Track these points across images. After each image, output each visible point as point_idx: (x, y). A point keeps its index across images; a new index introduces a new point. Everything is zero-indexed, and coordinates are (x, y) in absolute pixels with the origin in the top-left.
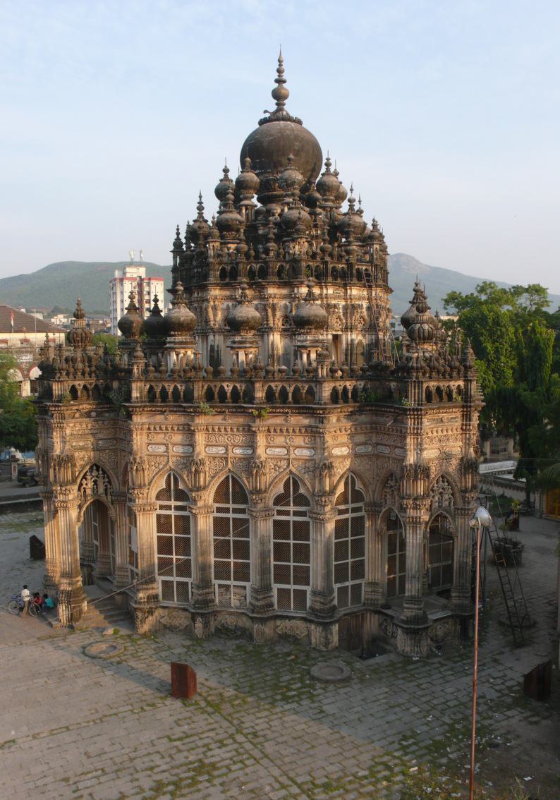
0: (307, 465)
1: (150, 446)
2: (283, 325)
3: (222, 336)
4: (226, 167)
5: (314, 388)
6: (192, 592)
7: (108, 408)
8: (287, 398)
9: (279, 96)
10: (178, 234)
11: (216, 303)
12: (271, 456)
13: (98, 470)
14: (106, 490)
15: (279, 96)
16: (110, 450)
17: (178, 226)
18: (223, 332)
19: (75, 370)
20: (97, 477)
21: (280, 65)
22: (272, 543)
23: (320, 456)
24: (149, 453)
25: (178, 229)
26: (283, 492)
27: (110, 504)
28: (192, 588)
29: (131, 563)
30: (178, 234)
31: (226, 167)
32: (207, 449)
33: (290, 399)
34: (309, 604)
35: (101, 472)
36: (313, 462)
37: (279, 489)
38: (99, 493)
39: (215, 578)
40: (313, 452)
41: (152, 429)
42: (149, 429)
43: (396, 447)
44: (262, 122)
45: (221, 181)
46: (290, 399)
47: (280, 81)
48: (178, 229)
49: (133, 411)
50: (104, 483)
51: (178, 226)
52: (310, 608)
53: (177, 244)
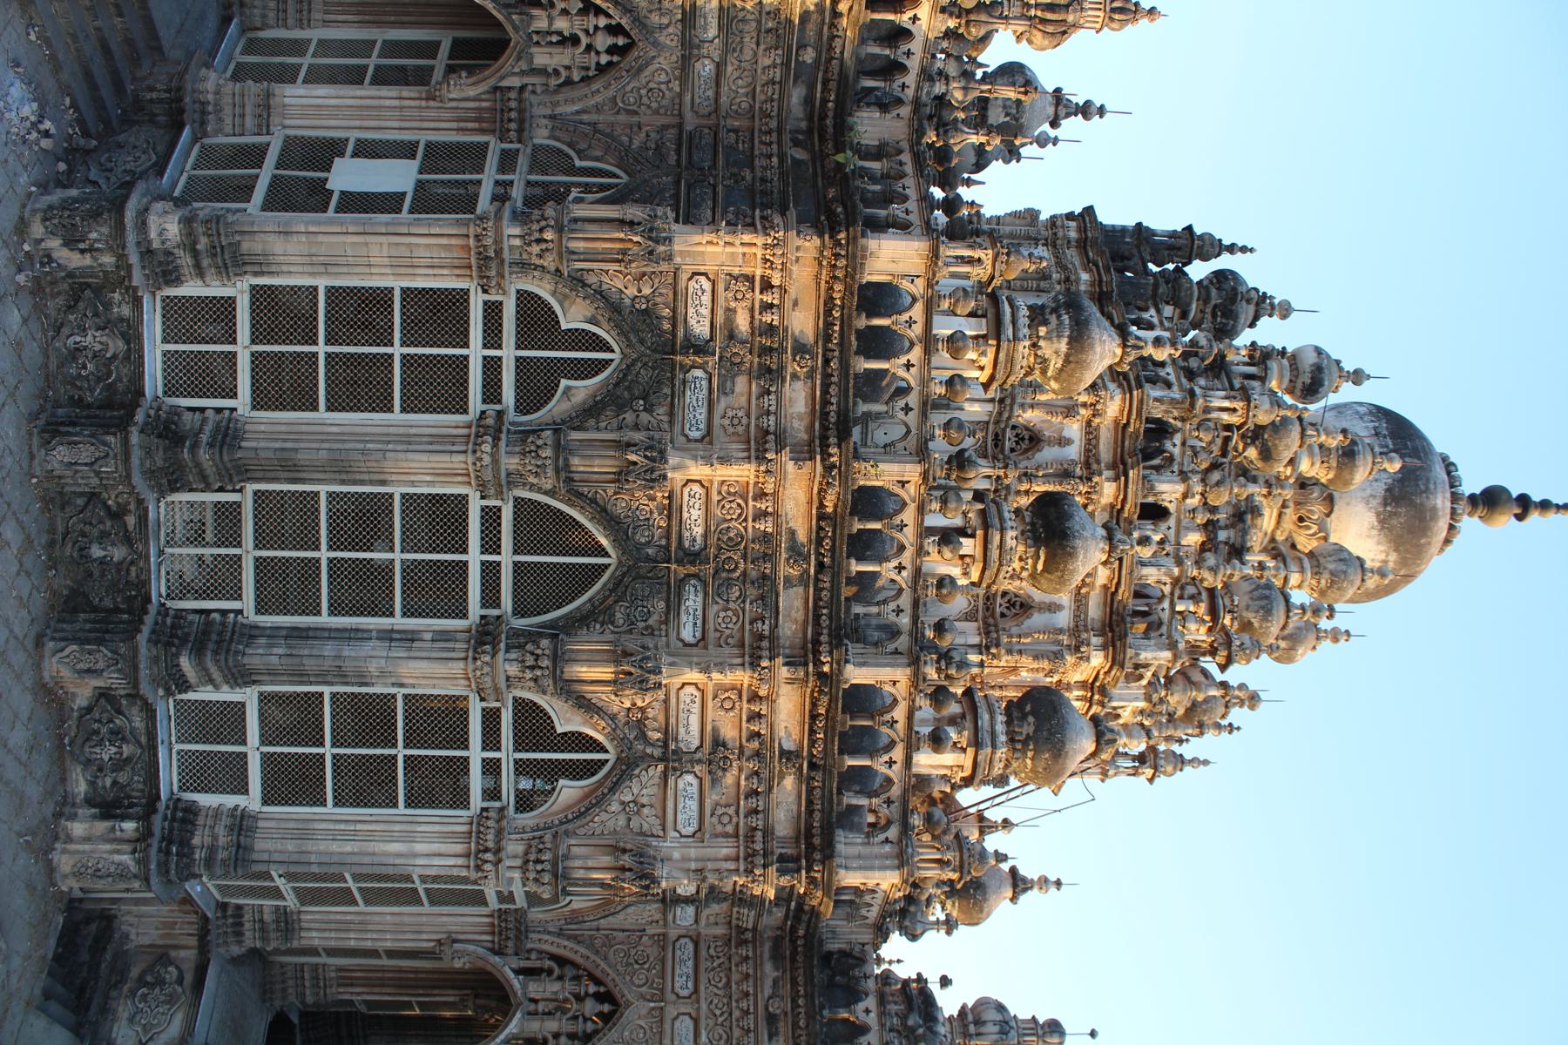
0: (646, 811)
1: (707, 285)
2: (1004, 594)
3: (986, 419)
4: (1369, 377)
5: (882, 837)
6: (202, 410)
7: (824, 101)
8: (854, 752)
9: (1490, 500)
10: (1231, 249)
11: (1083, 411)
12: (673, 700)
13: (611, 50)
14: (543, 72)
15: (1490, 500)
16: (680, 95)
17: (1251, 250)
18: (997, 422)
19: (969, 12)
20: (589, 48)
21: (1558, 507)
22: (393, 690)
23: (676, 855)
24: (684, 277)
25: (1244, 249)
26: (560, 730)
27: (492, 82)
28: (219, 410)
29: (290, 144)
30: (1231, 249)
31: (1369, 377)
32: (696, 488)
33: (851, 762)
34: (206, 800)
35: (604, 59)
36: (658, 831)
37: (569, 721)
38: (534, 50)
39: (256, 493)
40: (690, 830)
41: (768, 298)
42: (767, 286)
43: (696, 1021)
44: (1449, 467)
45: (1338, 362)
46: (851, 762)
47: (1524, 505)
48: (1244, 249)
49: (838, 243)
50: (568, 68)
51: (1251, 250)
52: (192, 810)
53: (1208, 247)
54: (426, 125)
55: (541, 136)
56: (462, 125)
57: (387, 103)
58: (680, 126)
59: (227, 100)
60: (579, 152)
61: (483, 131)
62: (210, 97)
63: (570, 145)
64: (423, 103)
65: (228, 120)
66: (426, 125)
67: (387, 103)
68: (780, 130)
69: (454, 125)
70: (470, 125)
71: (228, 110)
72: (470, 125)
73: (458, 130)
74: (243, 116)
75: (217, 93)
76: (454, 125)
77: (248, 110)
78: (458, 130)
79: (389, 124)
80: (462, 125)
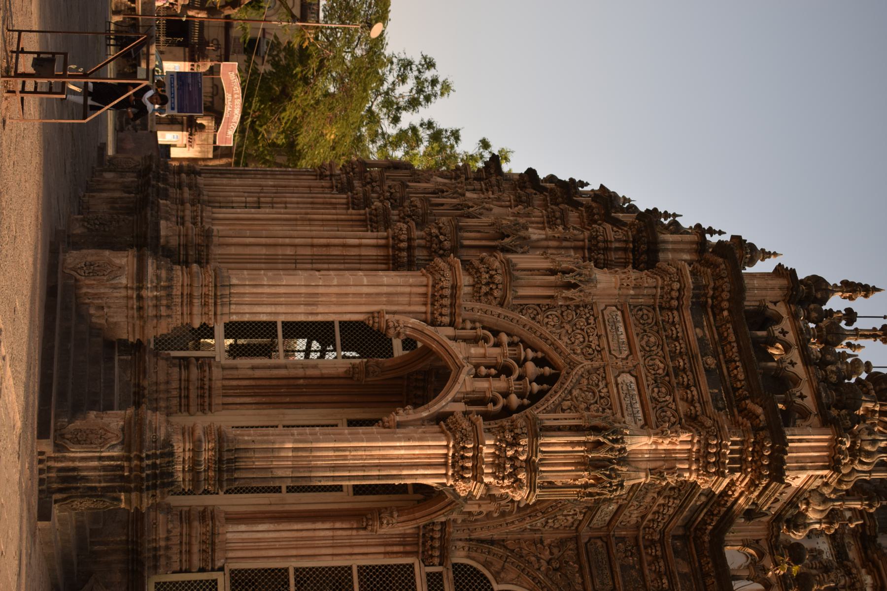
54: (356, 550)
55: (459, 557)
56: (389, 549)
57: (322, 533)
58: (577, 539)
59: (176, 540)
60: (496, 575)
61: (406, 554)
62: (162, 544)
63: (486, 565)
64: (354, 533)
65: (176, 558)
66: (356, 550)
67: (322, 533)
68: (662, 541)
69: (382, 549)
70: (396, 549)
71: (175, 549)
72: (396, 549)
73: (385, 553)
74: (189, 552)
75: (167, 539)
76: (382, 549)
77: (195, 548)
78: (385, 553)
79: (323, 551)
80: (389, 549)
